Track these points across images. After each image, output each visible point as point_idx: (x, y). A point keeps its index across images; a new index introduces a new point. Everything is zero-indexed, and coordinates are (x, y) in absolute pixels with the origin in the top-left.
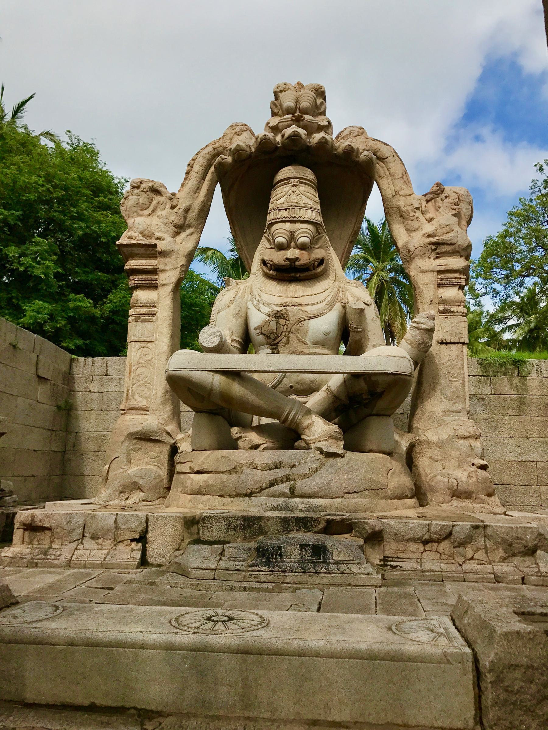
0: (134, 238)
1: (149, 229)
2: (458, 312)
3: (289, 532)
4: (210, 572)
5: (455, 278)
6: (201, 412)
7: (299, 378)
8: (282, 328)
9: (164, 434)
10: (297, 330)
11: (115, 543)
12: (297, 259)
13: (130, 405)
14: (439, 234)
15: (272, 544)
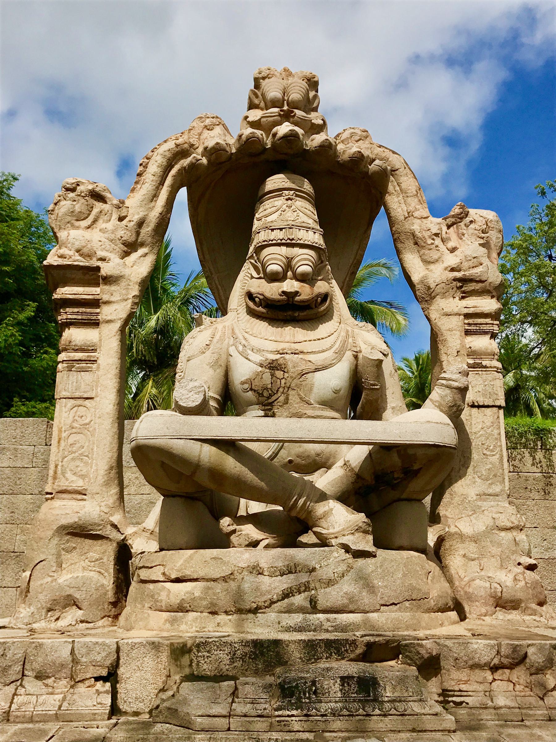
0: (68, 257)
1: (89, 246)
2: (491, 367)
3: (316, 660)
4: (223, 720)
5: (487, 324)
6: (174, 496)
7: (301, 450)
8: (279, 383)
9: (109, 527)
10: (299, 386)
11: (73, 683)
12: (296, 293)
13: (59, 486)
14: (464, 268)
15: (302, 678)
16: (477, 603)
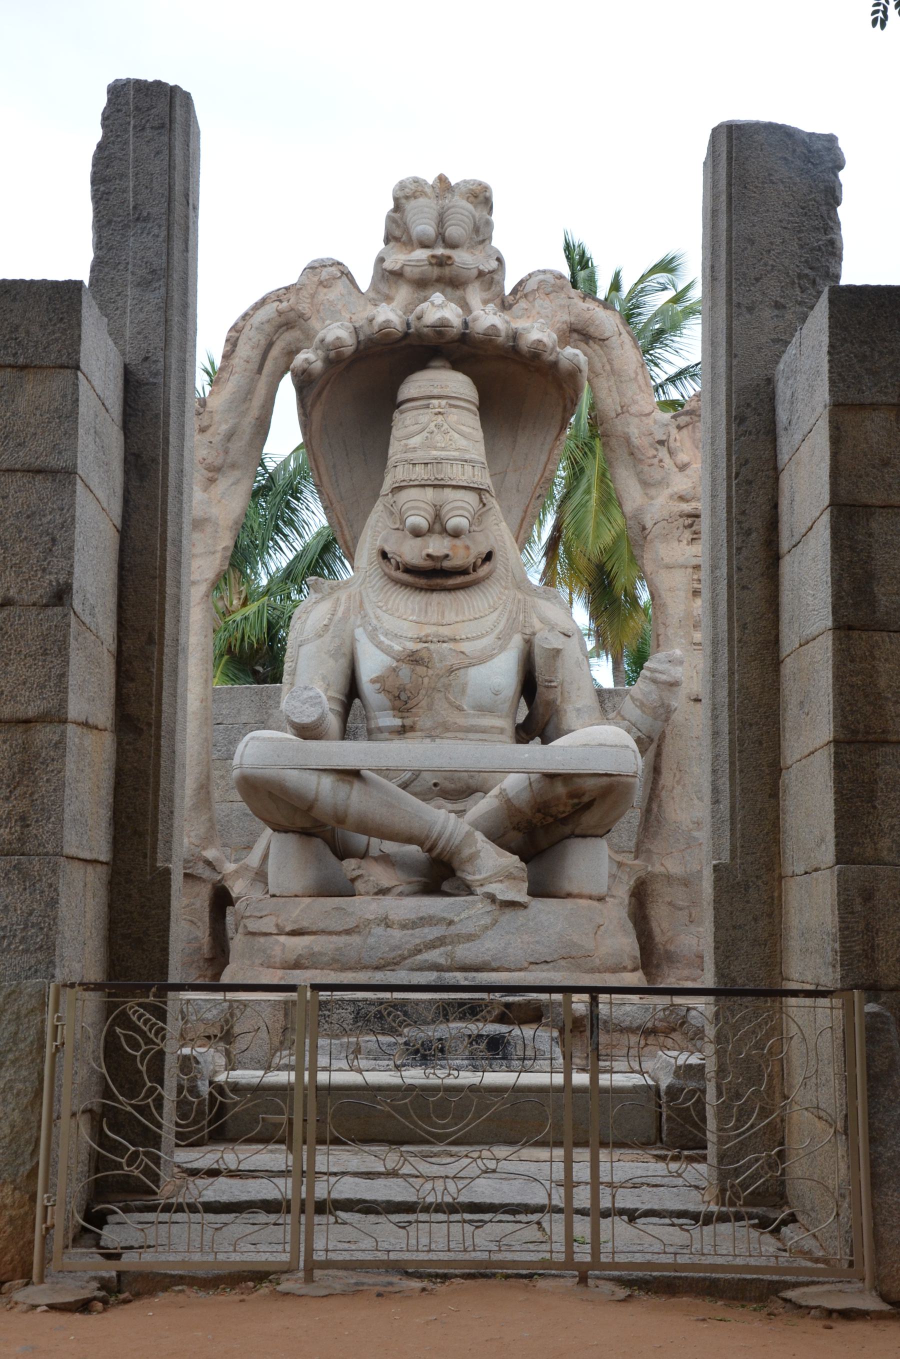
6: (286, 832)
10: (447, 687)
12: (447, 556)
16: (679, 965)
